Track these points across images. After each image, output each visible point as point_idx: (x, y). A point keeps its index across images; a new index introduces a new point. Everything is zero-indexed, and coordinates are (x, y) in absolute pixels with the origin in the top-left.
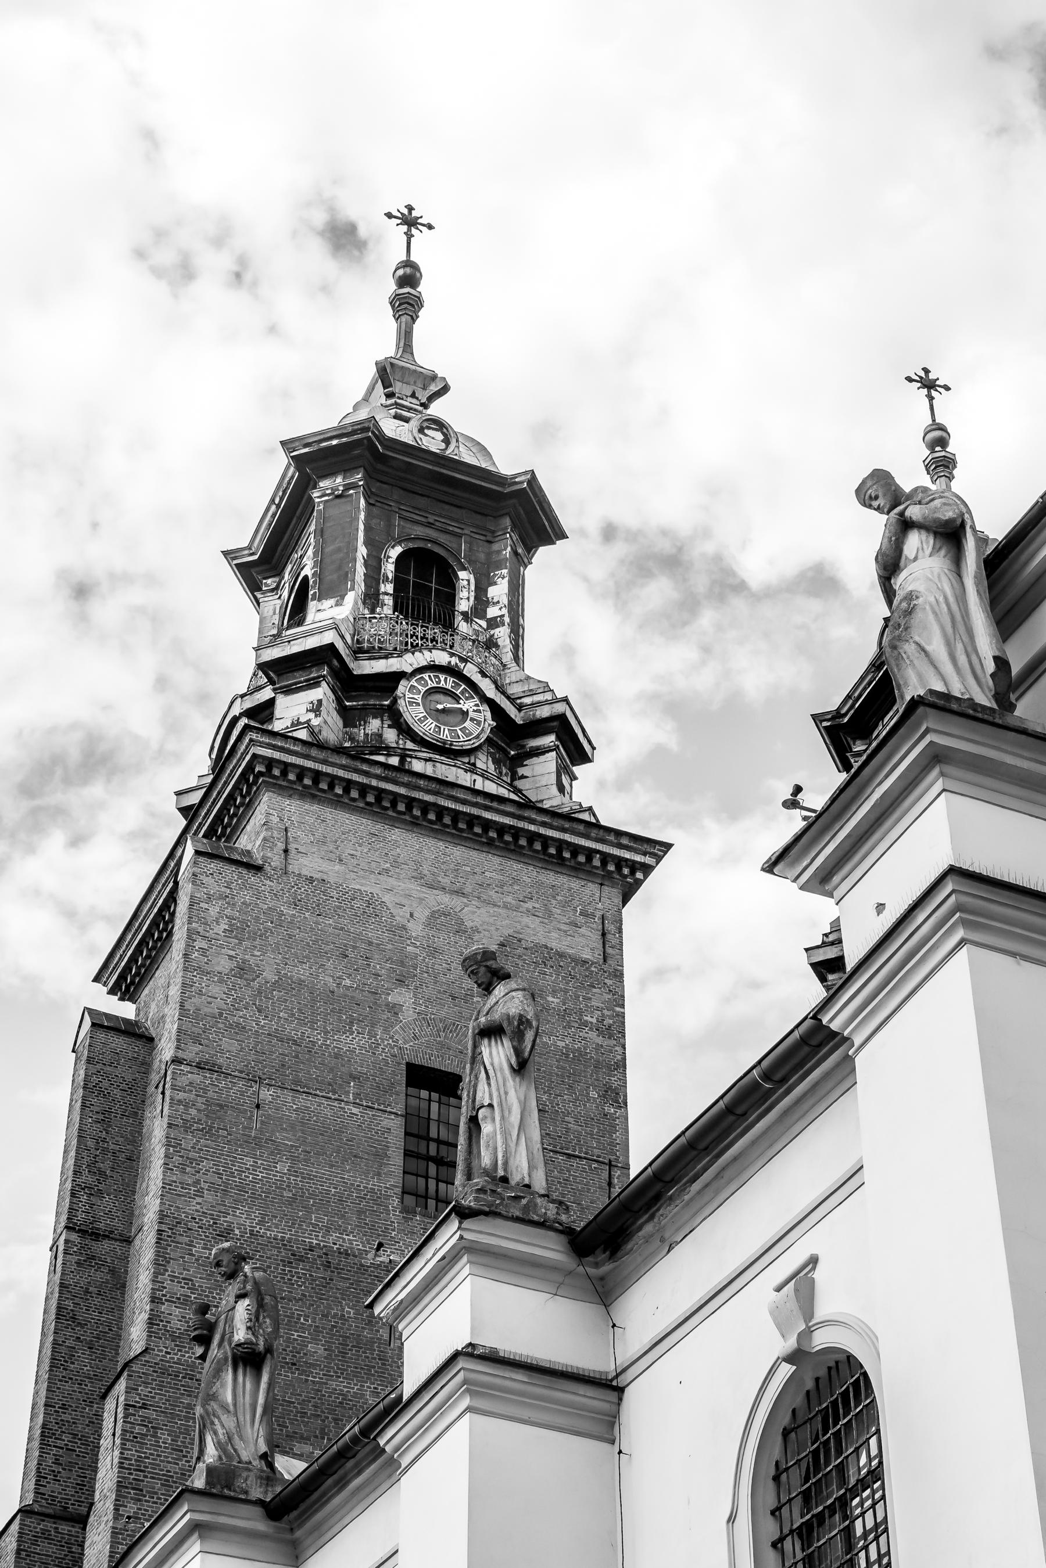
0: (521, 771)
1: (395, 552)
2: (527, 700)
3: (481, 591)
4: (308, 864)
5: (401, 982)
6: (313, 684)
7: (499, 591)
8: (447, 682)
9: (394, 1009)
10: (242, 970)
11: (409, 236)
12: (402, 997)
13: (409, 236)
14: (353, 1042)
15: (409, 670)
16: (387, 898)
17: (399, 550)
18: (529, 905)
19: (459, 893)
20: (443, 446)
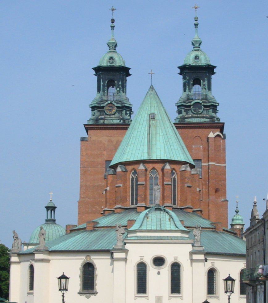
0: (123, 112)
1: (106, 82)
2: (122, 102)
3: (118, 83)
4: (94, 138)
5: (104, 150)
6: (94, 110)
7: (120, 83)
8: (111, 105)
9: (104, 154)
10: (87, 154)
11: (113, 13)
12: (105, 153)
13: (113, 13)
14: (99, 160)
15: (105, 105)
16: (103, 140)
17: (107, 81)
18: (120, 135)
19: (111, 137)
20: (112, 61)
